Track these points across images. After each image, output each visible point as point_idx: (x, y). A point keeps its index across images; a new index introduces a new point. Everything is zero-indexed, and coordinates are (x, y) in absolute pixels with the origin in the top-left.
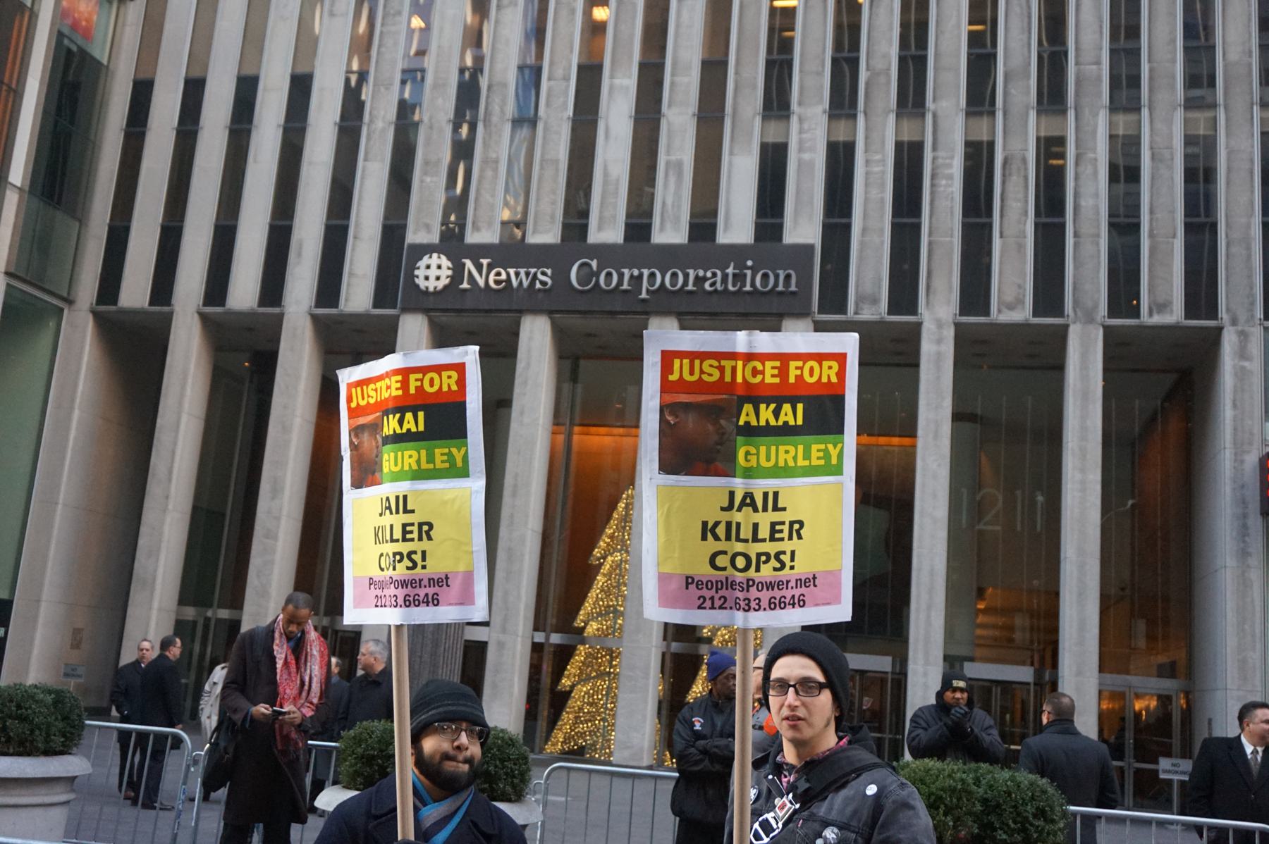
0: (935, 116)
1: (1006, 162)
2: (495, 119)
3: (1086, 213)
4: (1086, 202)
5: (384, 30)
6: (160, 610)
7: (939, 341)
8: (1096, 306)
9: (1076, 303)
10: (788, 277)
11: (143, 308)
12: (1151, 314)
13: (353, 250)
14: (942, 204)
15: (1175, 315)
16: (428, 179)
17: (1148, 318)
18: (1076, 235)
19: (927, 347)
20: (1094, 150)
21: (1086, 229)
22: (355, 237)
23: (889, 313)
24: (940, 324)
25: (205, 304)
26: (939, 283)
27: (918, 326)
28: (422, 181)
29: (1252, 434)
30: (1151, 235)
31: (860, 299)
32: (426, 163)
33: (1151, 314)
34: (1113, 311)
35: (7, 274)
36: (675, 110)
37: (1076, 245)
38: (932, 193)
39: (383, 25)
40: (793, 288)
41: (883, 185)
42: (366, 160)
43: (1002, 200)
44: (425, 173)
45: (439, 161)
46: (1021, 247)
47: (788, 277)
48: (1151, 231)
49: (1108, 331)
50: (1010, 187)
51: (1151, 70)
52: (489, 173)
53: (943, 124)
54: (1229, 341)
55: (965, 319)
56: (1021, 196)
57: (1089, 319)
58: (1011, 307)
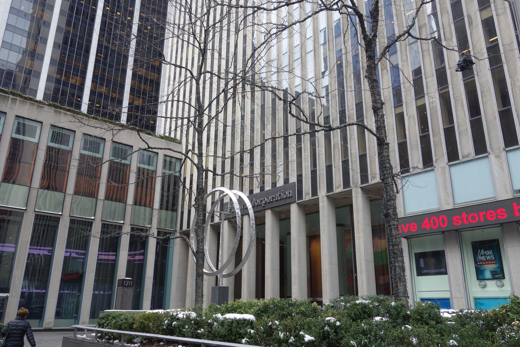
0: (318, 138)
1: (334, 145)
2: (237, 168)
3: (353, 155)
7: (323, 202)
8: (358, 182)
9: (353, 182)
10: (290, 192)
12: (371, 181)
14: (321, 162)
17: (372, 182)
18: (352, 162)
19: (321, 204)
20: (354, 135)
21: (354, 160)
24: (323, 197)
26: (322, 185)
29: (401, 212)
30: (370, 157)
31: (306, 194)
33: (371, 181)
34: (362, 183)
35: (157, 228)
36: (267, 154)
37: (352, 165)
38: (319, 160)
40: (291, 195)
41: (308, 161)
43: (334, 157)
46: (339, 169)
47: (290, 192)
48: (369, 155)
49: (362, 188)
50: (335, 153)
51: (366, 107)
52: (236, 181)
53: (320, 140)
56: (338, 154)
58: (338, 188)
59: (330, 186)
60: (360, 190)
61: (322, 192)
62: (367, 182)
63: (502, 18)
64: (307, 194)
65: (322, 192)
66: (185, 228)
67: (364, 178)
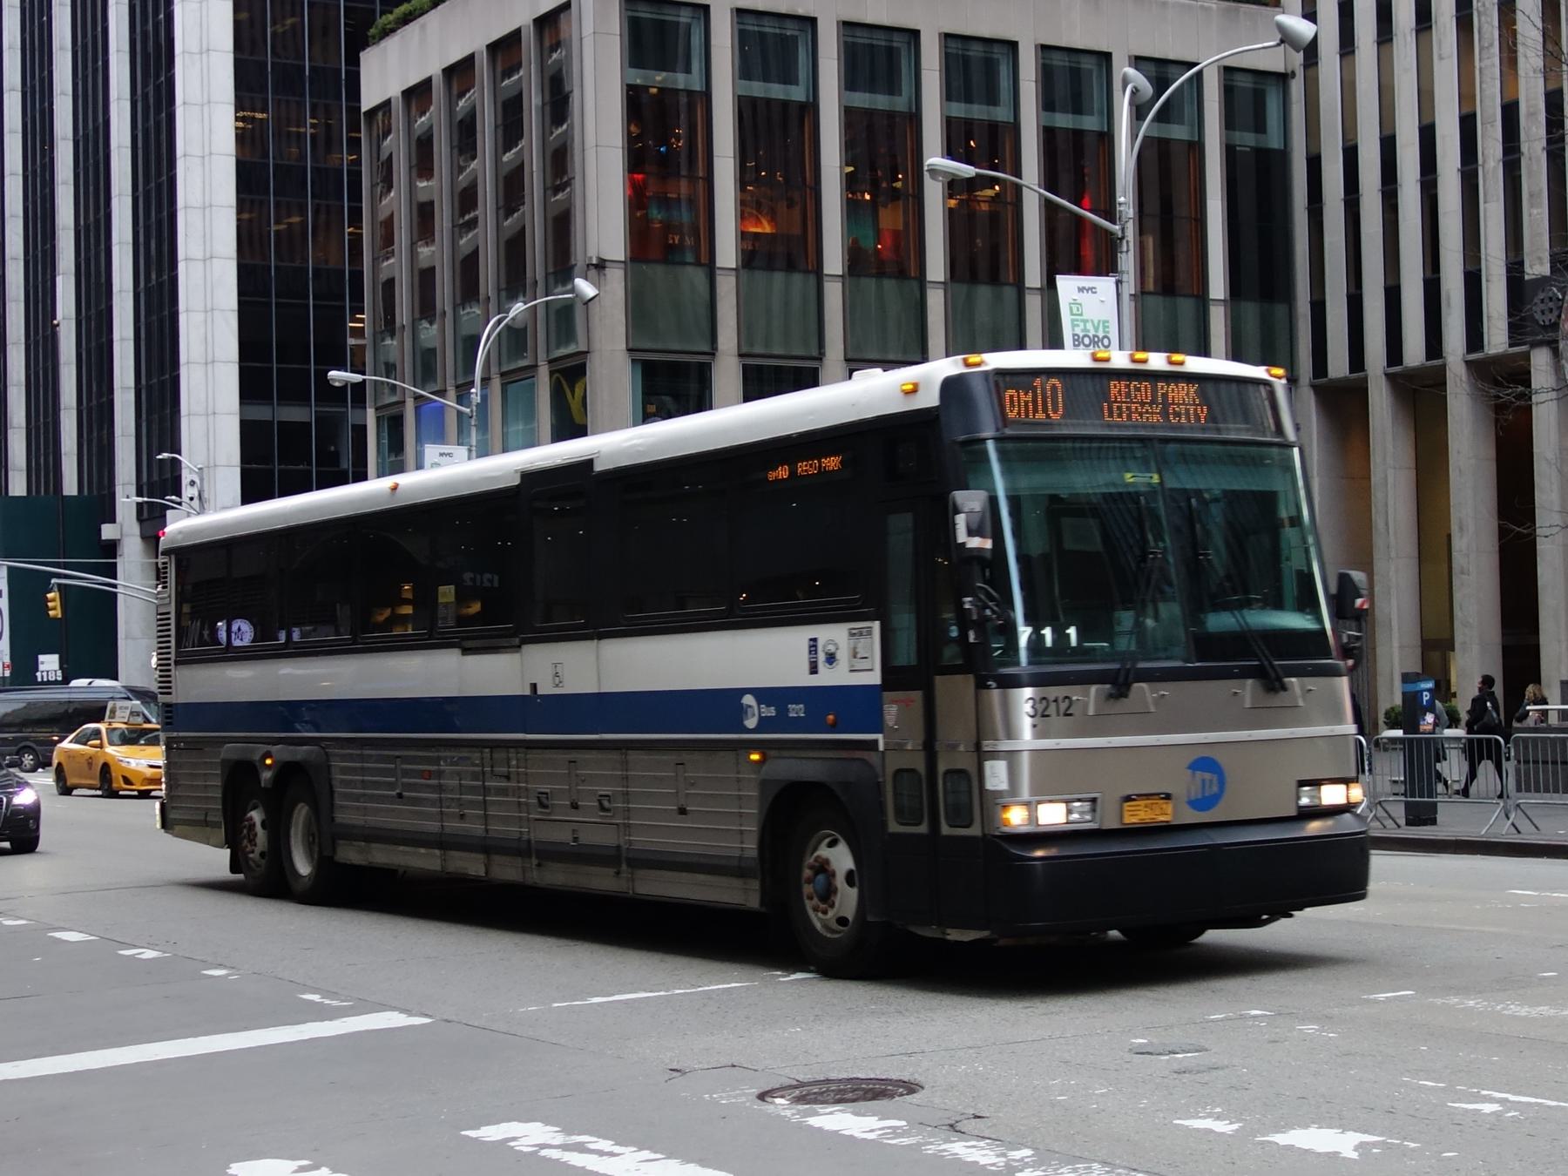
5: (1483, 66)
6: (1401, 647)
11: (1346, 377)
13: (1487, 293)
16: (1535, 211)
22: (1487, 281)
25: (1389, 366)
28: (1530, 215)
32: (1531, 195)
39: (1480, 60)
42: (1485, 202)
44: (1532, 206)
45: (1541, 190)
66: (1338, 365)
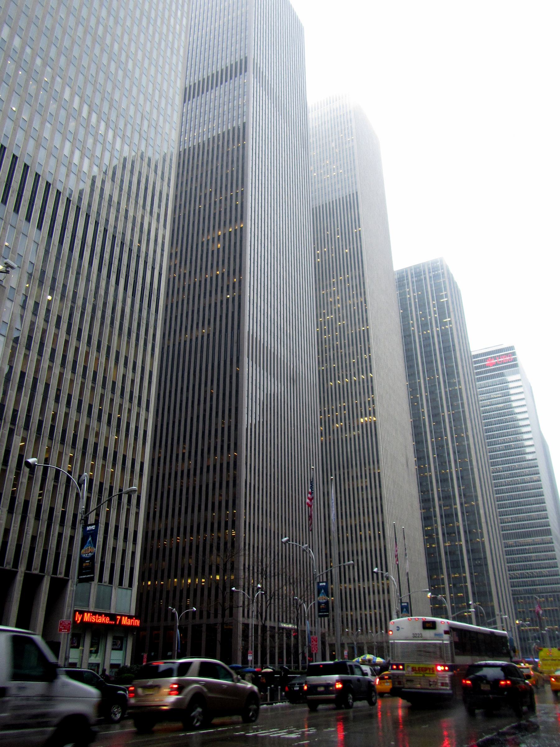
4: (52, 546)
15: (62, 576)
17: (59, 576)
23: (12, 568)
27: (17, 572)
34: (53, 574)
49: (52, 578)
53: (30, 520)
54: (70, 582)
55: (27, 571)
57: (48, 575)
58: (36, 569)
59: (29, 566)
60: (49, 578)
61: (22, 569)
62: (56, 575)
63: (132, 516)
64: (8, 563)
65: (22, 569)
67: (55, 571)
